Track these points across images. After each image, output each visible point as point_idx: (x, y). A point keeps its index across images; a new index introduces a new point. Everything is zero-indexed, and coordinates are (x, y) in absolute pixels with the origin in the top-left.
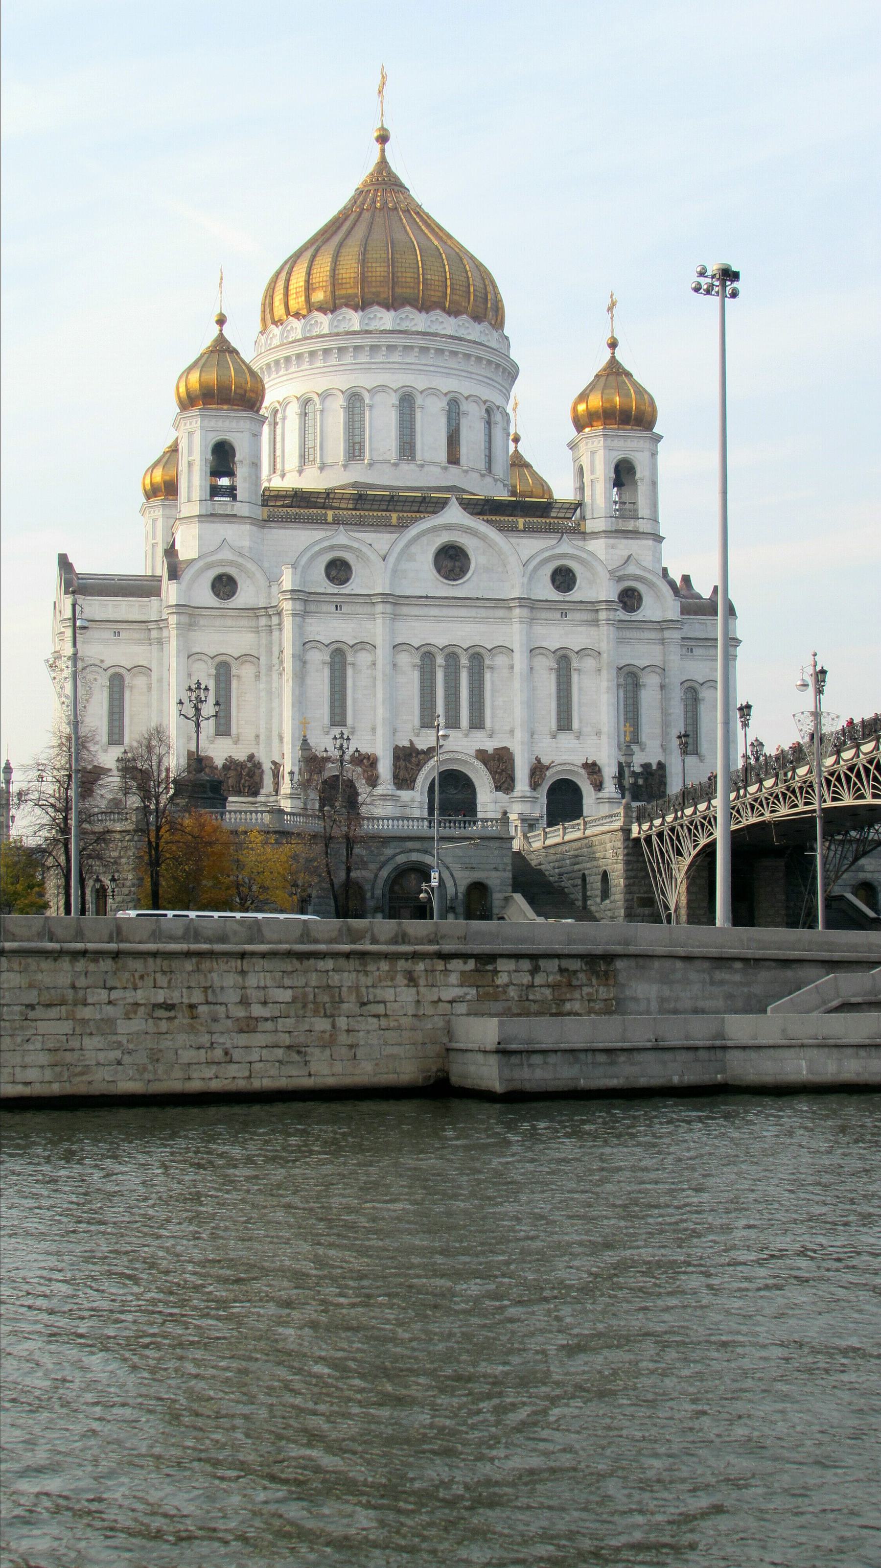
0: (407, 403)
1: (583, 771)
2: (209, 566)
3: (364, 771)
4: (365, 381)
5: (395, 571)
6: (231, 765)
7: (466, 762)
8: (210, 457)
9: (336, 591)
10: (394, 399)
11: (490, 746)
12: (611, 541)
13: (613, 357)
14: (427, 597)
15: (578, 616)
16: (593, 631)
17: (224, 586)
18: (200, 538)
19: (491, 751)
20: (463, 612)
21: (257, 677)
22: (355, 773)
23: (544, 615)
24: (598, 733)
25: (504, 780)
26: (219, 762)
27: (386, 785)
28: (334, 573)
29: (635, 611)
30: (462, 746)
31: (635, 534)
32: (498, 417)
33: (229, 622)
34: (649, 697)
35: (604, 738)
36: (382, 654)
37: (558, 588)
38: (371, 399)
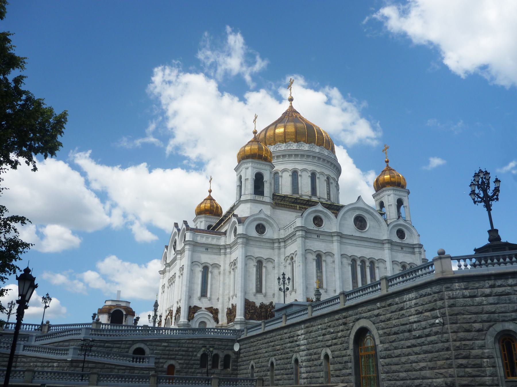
0: (313, 176)
2: (255, 220)
5: (340, 224)
6: (262, 305)
8: (254, 178)
9: (317, 229)
10: (310, 174)
13: (388, 166)
16: (413, 256)
17: (260, 229)
18: (251, 208)
20: (366, 244)
21: (274, 268)
23: (395, 248)
26: (258, 305)
28: (316, 222)
33: (262, 244)
36: (337, 257)
38: (301, 173)
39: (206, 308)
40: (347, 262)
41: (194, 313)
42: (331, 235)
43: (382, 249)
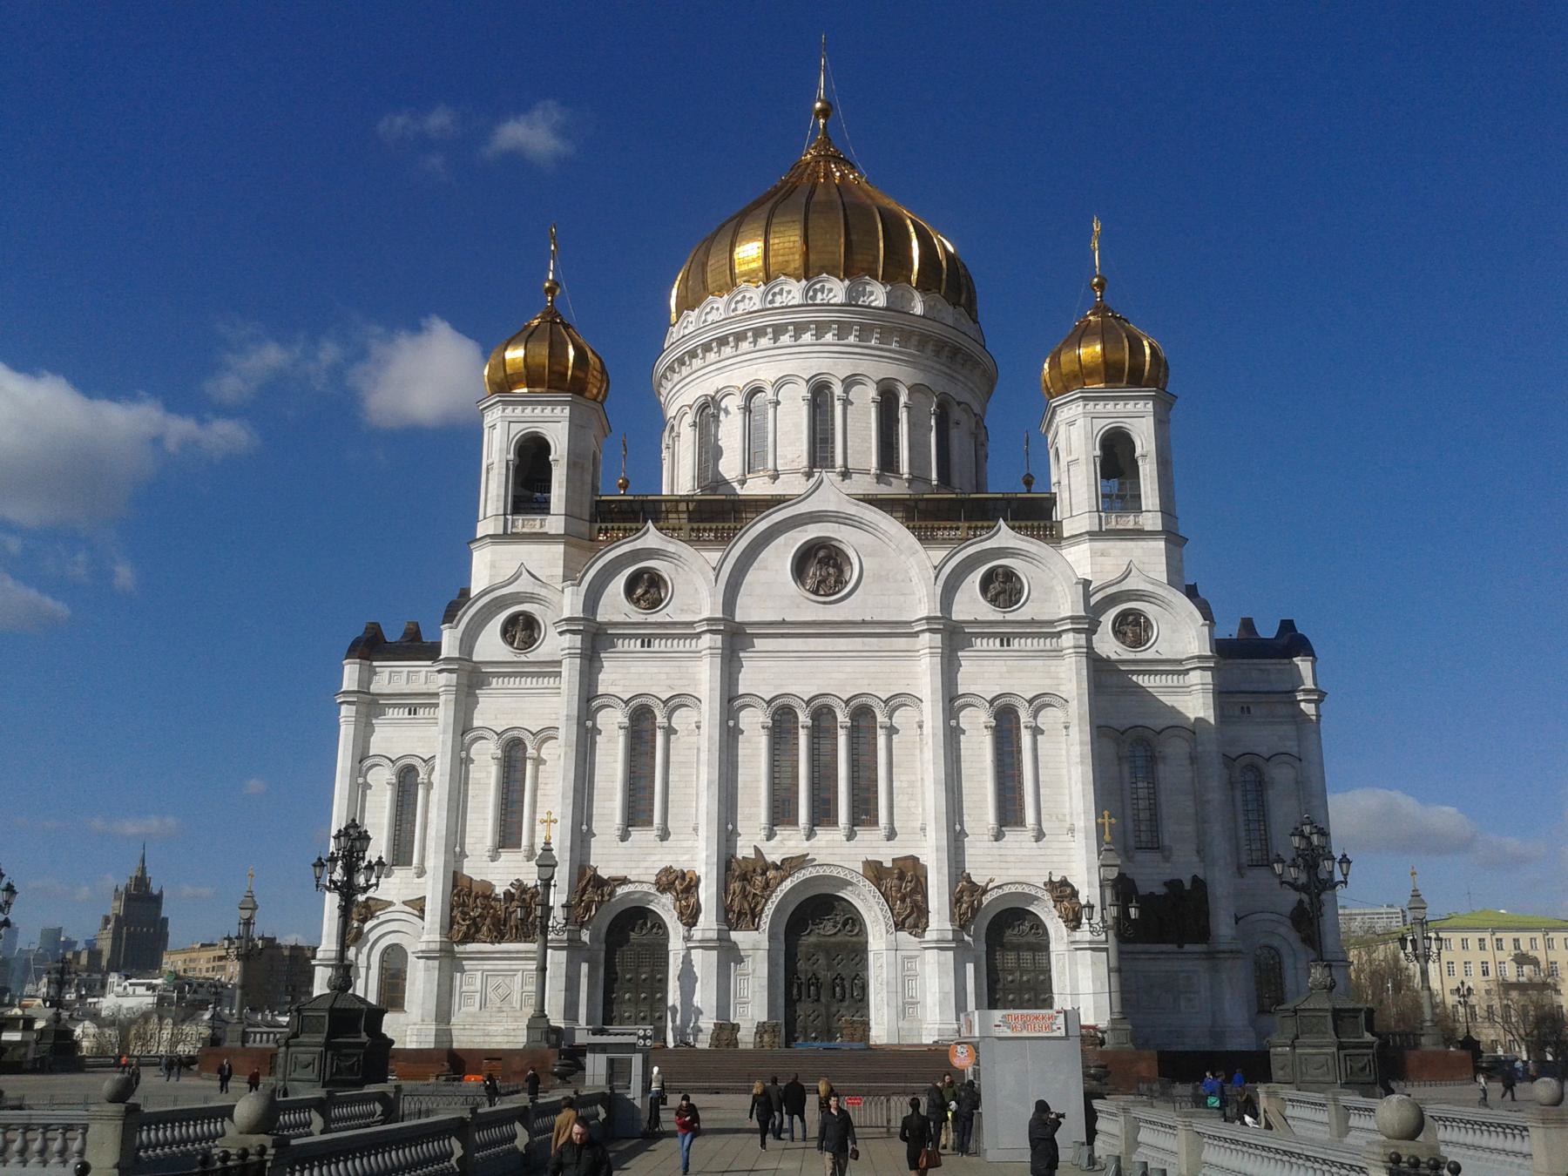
0: (819, 395)
1: (1047, 896)
3: (677, 899)
4: (766, 373)
7: (846, 883)
11: (886, 854)
12: (1099, 545)
14: (784, 622)
15: (1029, 643)
17: (522, 630)
18: (493, 565)
19: (888, 864)
20: (842, 644)
22: (665, 907)
24: (1072, 830)
25: (911, 916)
27: (708, 922)
29: (1141, 645)
30: (837, 852)
31: (1138, 534)
32: (956, 413)
34: (1174, 773)
35: (1080, 836)
37: (993, 601)
39: (405, 903)
40: (754, 723)
41: (364, 921)
42: (685, 631)
43: (910, 654)
